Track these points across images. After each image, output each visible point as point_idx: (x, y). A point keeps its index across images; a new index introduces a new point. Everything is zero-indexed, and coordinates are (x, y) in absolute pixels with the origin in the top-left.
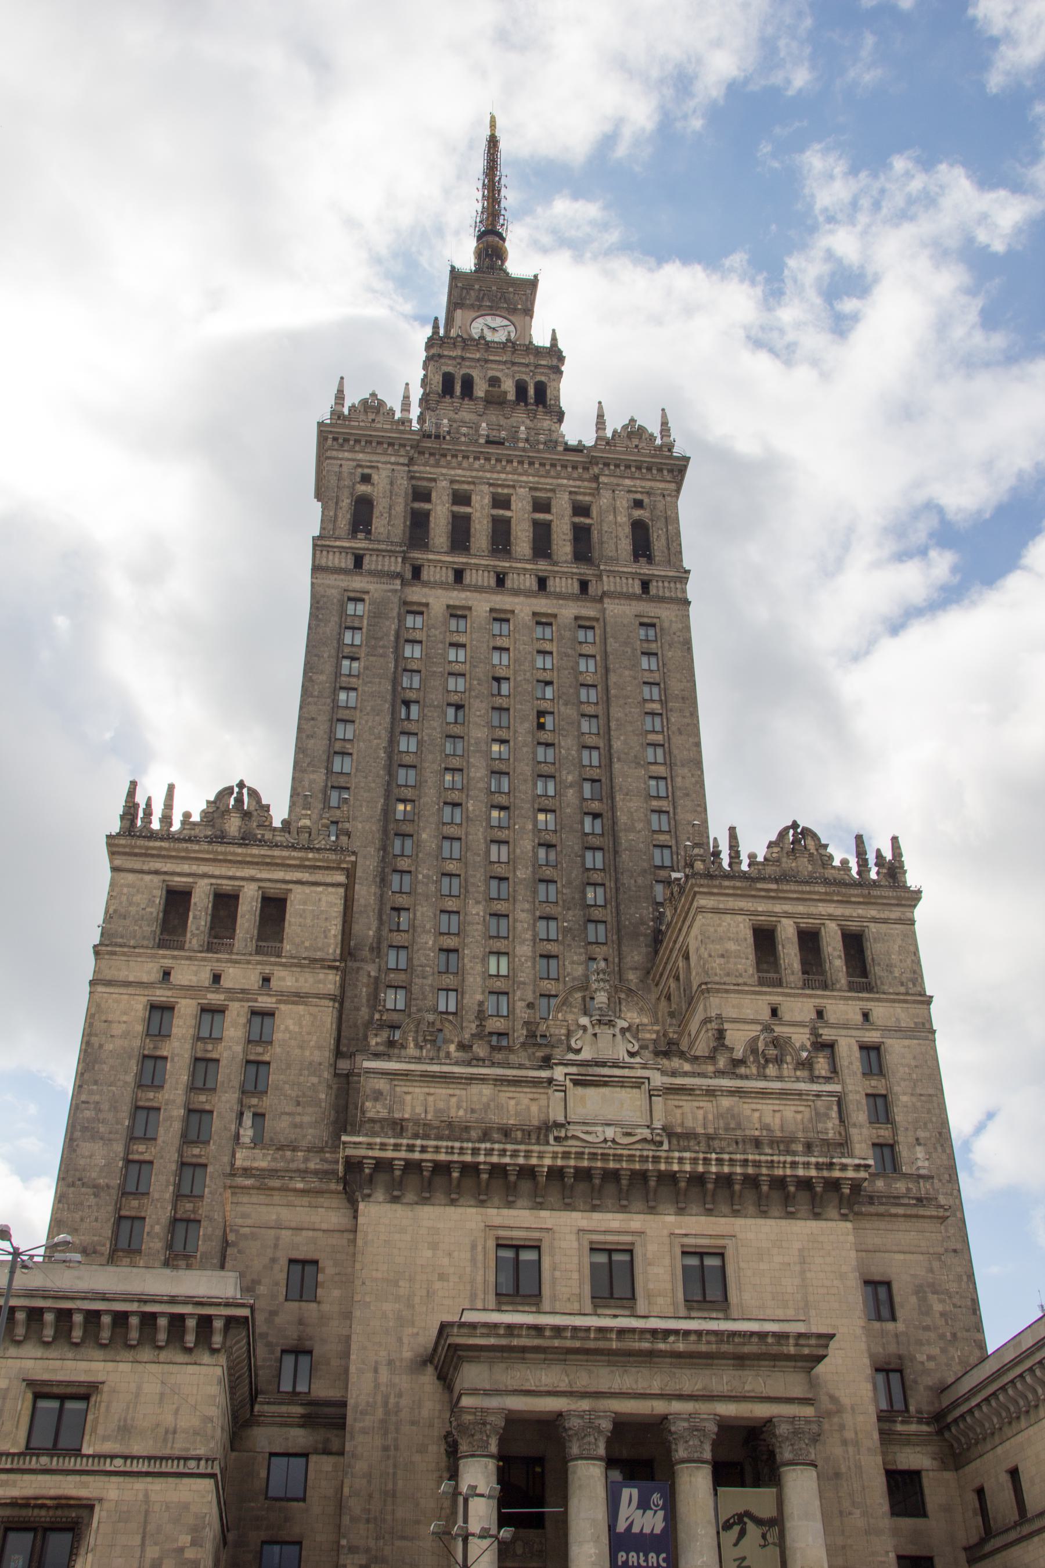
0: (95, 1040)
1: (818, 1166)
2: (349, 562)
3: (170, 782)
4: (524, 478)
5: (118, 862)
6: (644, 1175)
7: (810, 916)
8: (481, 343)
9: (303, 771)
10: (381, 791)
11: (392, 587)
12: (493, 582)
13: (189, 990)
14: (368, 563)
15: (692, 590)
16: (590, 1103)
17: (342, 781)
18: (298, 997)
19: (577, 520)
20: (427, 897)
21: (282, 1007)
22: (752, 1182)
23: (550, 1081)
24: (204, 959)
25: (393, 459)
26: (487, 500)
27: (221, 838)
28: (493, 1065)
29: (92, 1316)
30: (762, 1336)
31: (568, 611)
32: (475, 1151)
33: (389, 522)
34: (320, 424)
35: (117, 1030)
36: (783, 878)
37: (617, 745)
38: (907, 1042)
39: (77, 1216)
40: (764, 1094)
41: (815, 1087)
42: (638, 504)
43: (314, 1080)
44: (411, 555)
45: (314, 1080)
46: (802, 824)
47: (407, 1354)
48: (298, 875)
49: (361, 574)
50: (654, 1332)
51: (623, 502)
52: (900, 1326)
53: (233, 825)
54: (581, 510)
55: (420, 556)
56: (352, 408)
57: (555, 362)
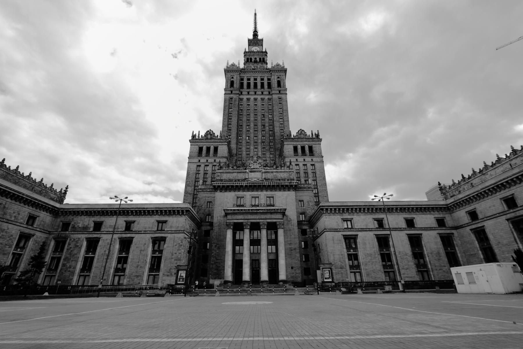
2: (230, 92)
6: (260, 185)
16: (252, 175)
22: (278, 186)
27: (207, 139)
29: (165, 211)
30: (274, 209)
31: (266, 97)
33: (237, 85)
35: (192, 170)
36: (299, 138)
40: (281, 172)
42: (278, 78)
50: (257, 210)
51: (276, 77)
53: (209, 136)
54: (269, 79)
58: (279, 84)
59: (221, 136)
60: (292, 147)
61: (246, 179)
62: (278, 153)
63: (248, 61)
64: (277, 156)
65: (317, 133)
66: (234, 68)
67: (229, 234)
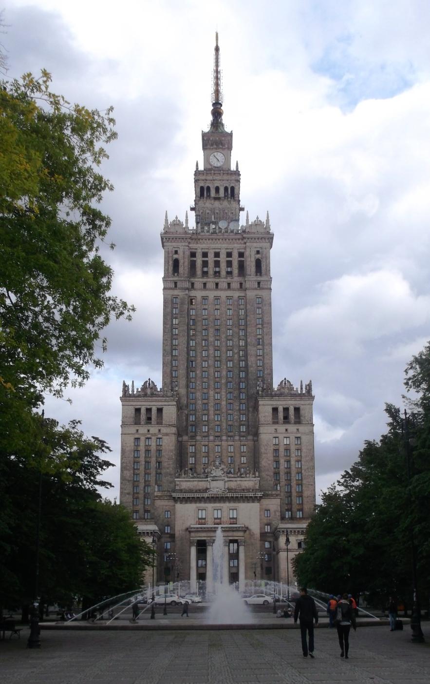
0: (124, 448)
1: (253, 494)
4: (223, 245)
5: (123, 404)
6: (223, 497)
7: (286, 404)
9: (165, 356)
10: (186, 361)
11: (185, 293)
12: (215, 286)
13: (143, 435)
14: (179, 285)
15: (274, 285)
16: (214, 484)
17: (175, 358)
18: (167, 435)
20: (199, 390)
21: (164, 437)
23: (207, 480)
25: (184, 244)
26: (213, 255)
27: (145, 395)
28: (198, 478)
30: (236, 527)
31: (236, 294)
32: (194, 495)
33: (184, 268)
35: (128, 445)
37: (249, 340)
38: (307, 436)
39: (125, 487)
41: (255, 479)
43: (172, 454)
44: (191, 280)
45: (172, 454)
46: (287, 379)
47: (184, 528)
48: (166, 403)
49: (176, 289)
52: (270, 518)
53: (149, 391)
54: (241, 255)
58: (258, 263)
61: (207, 489)
62: (252, 404)
63: (202, 192)
64: (251, 409)
66: (180, 230)
67: (193, 550)
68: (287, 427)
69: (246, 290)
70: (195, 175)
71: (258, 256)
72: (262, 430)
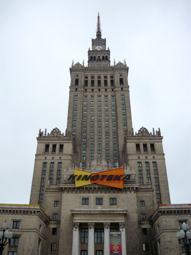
2: (74, 90)
3: (46, 128)
5: (38, 142)
7: (145, 142)
8: (96, 51)
12: (98, 91)
19: (111, 79)
24: (51, 155)
27: (53, 137)
34: (70, 68)
42: (121, 75)
46: (144, 127)
51: (119, 75)
53: (55, 134)
54: (112, 77)
55: (86, 88)
56: (75, 65)
57: (109, 53)
58: (121, 81)
59: (66, 134)
60: (134, 145)
63: (91, 59)
65: (158, 130)
68: (146, 156)
69: (115, 91)
70: (88, 52)
71: (121, 77)
72: (129, 157)
